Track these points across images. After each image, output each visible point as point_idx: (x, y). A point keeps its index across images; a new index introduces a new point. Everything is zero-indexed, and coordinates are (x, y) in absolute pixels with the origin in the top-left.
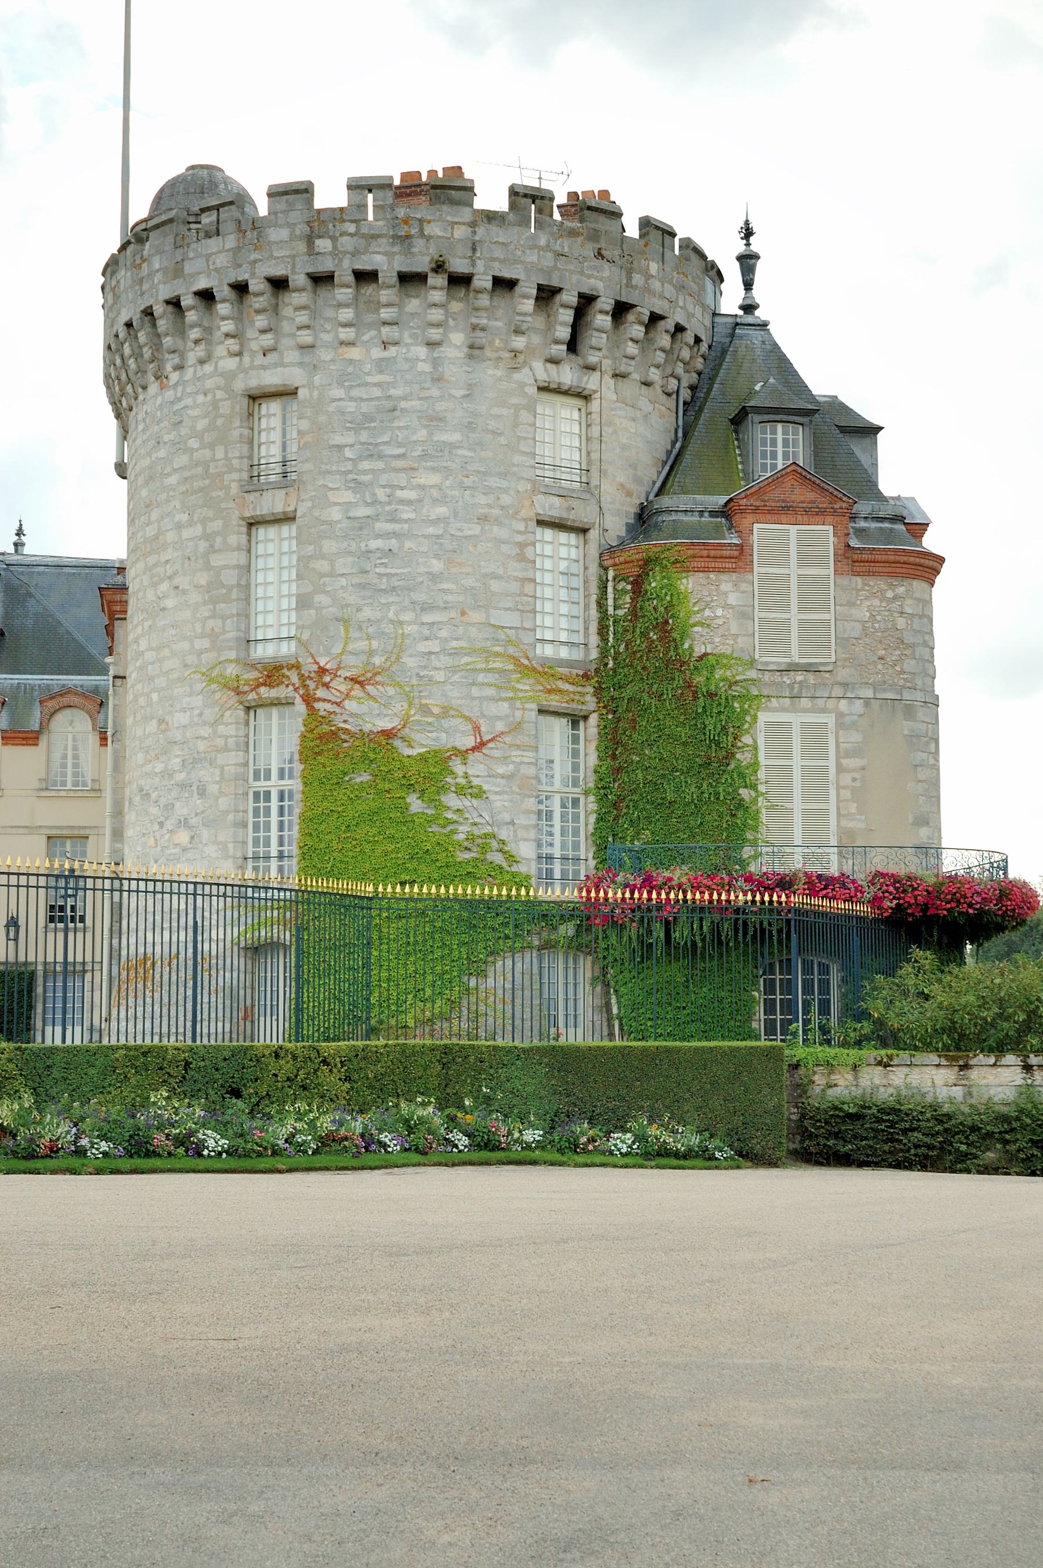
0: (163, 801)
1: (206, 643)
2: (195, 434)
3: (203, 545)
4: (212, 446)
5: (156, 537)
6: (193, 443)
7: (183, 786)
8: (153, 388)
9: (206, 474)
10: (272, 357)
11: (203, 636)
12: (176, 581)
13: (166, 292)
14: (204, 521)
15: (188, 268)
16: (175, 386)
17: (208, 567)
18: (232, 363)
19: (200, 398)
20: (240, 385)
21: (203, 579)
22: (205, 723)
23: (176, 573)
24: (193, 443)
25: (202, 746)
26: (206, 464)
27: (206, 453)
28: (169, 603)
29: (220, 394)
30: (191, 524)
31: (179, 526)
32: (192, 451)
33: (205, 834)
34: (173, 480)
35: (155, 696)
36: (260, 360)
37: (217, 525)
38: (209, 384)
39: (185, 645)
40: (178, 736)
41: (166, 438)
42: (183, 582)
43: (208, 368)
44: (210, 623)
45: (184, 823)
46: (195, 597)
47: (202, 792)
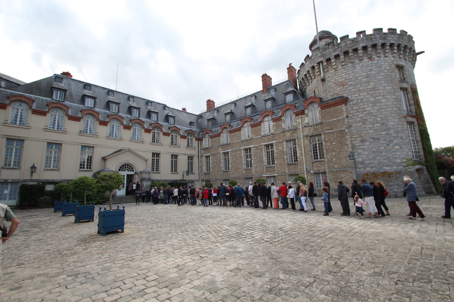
0: (387, 140)
1: (397, 109)
2: (385, 69)
3: (393, 91)
4: (391, 72)
5: (374, 88)
6: (385, 71)
7: (395, 137)
8: (366, 60)
9: (391, 77)
10: (400, 60)
11: (396, 108)
12: (385, 97)
13: (381, 42)
14: (392, 86)
15: (388, 38)
16: (377, 60)
17: (395, 95)
18: (393, 59)
19: (386, 63)
20: (395, 63)
21: (394, 97)
22: (399, 125)
23: (385, 95)
24: (385, 71)
25: (400, 129)
26: (391, 76)
27: (390, 74)
28: (383, 101)
29: (391, 64)
30: (388, 86)
31: (385, 86)
32: (386, 73)
33: (404, 147)
34: (380, 77)
35: (379, 119)
36: (398, 59)
37: (395, 87)
38: (389, 61)
39: (391, 109)
40: (392, 127)
41: (375, 70)
42: (388, 97)
43: (387, 58)
44: (398, 106)
45: (398, 144)
46: (392, 100)
47: (402, 138)
